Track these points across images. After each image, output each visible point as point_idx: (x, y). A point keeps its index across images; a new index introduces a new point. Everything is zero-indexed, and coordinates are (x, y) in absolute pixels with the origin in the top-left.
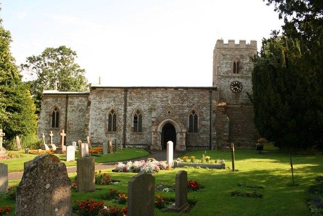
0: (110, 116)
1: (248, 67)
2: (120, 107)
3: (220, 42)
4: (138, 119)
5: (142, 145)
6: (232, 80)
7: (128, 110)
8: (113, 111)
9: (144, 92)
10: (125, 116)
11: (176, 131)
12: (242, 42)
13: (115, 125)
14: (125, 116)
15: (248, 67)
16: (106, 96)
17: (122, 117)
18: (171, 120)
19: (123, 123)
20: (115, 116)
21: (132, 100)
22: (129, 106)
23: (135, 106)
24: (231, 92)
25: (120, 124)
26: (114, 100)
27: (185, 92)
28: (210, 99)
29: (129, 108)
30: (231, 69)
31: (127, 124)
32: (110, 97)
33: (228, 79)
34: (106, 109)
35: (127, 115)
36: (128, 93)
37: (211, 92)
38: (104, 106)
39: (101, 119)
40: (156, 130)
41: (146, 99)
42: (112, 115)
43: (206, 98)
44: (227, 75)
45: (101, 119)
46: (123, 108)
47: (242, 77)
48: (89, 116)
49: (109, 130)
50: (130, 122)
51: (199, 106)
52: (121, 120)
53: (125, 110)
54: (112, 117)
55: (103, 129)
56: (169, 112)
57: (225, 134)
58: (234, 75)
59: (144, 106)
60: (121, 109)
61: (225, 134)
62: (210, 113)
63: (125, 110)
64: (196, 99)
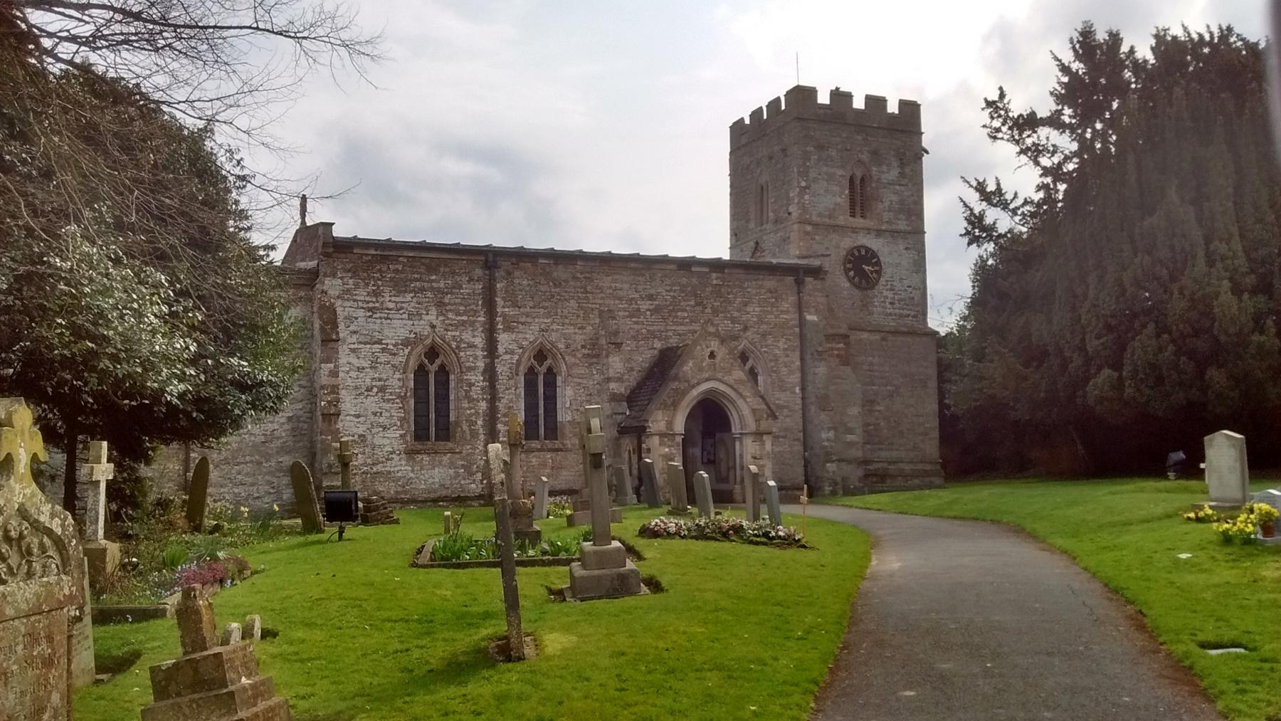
0: (421, 372)
1: (895, 198)
2: (467, 336)
3: (837, 89)
4: (541, 380)
5: (851, 507)
6: (847, 243)
7: (501, 349)
8: (432, 353)
9: (561, 272)
10: (490, 374)
11: (736, 429)
12: (875, 103)
13: (443, 412)
14: (490, 374)
15: (895, 198)
16: (400, 287)
17: (477, 378)
18: (722, 387)
19: (483, 405)
20: (443, 372)
21: (515, 305)
22: (508, 329)
23: (530, 335)
24: (847, 285)
25: (468, 404)
26: (440, 305)
27: (715, 278)
28: (800, 308)
29: (504, 339)
30: (842, 199)
31: (501, 406)
32: (422, 290)
33: (834, 237)
34: (406, 342)
35: (499, 369)
36: (499, 274)
37: (799, 283)
38: (398, 329)
39: (382, 389)
40: (670, 424)
41: (573, 303)
42: (433, 368)
43: (785, 305)
44: (832, 222)
45: (382, 389)
46: (479, 341)
47: (879, 233)
48: (334, 374)
49: (421, 434)
50: (513, 400)
51: (764, 335)
52: (476, 392)
53: (491, 348)
54: (541, 378)
55: (395, 434)
56: (712, 355)
57: (850, 438)
58: (859, 222)
59: (565, 332)
60: (471, 346)
61: (850, 438)
62: (802, 359)
63: (491, 348)
64: (754, 309)
